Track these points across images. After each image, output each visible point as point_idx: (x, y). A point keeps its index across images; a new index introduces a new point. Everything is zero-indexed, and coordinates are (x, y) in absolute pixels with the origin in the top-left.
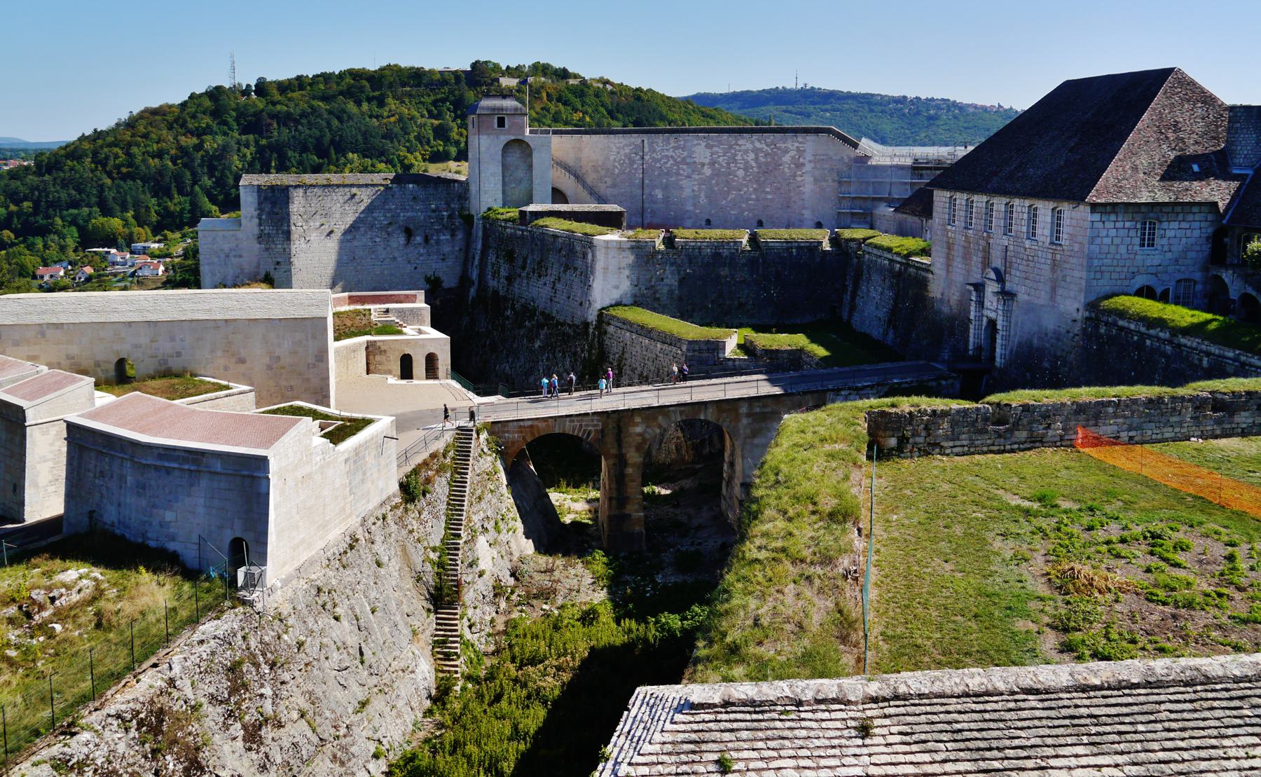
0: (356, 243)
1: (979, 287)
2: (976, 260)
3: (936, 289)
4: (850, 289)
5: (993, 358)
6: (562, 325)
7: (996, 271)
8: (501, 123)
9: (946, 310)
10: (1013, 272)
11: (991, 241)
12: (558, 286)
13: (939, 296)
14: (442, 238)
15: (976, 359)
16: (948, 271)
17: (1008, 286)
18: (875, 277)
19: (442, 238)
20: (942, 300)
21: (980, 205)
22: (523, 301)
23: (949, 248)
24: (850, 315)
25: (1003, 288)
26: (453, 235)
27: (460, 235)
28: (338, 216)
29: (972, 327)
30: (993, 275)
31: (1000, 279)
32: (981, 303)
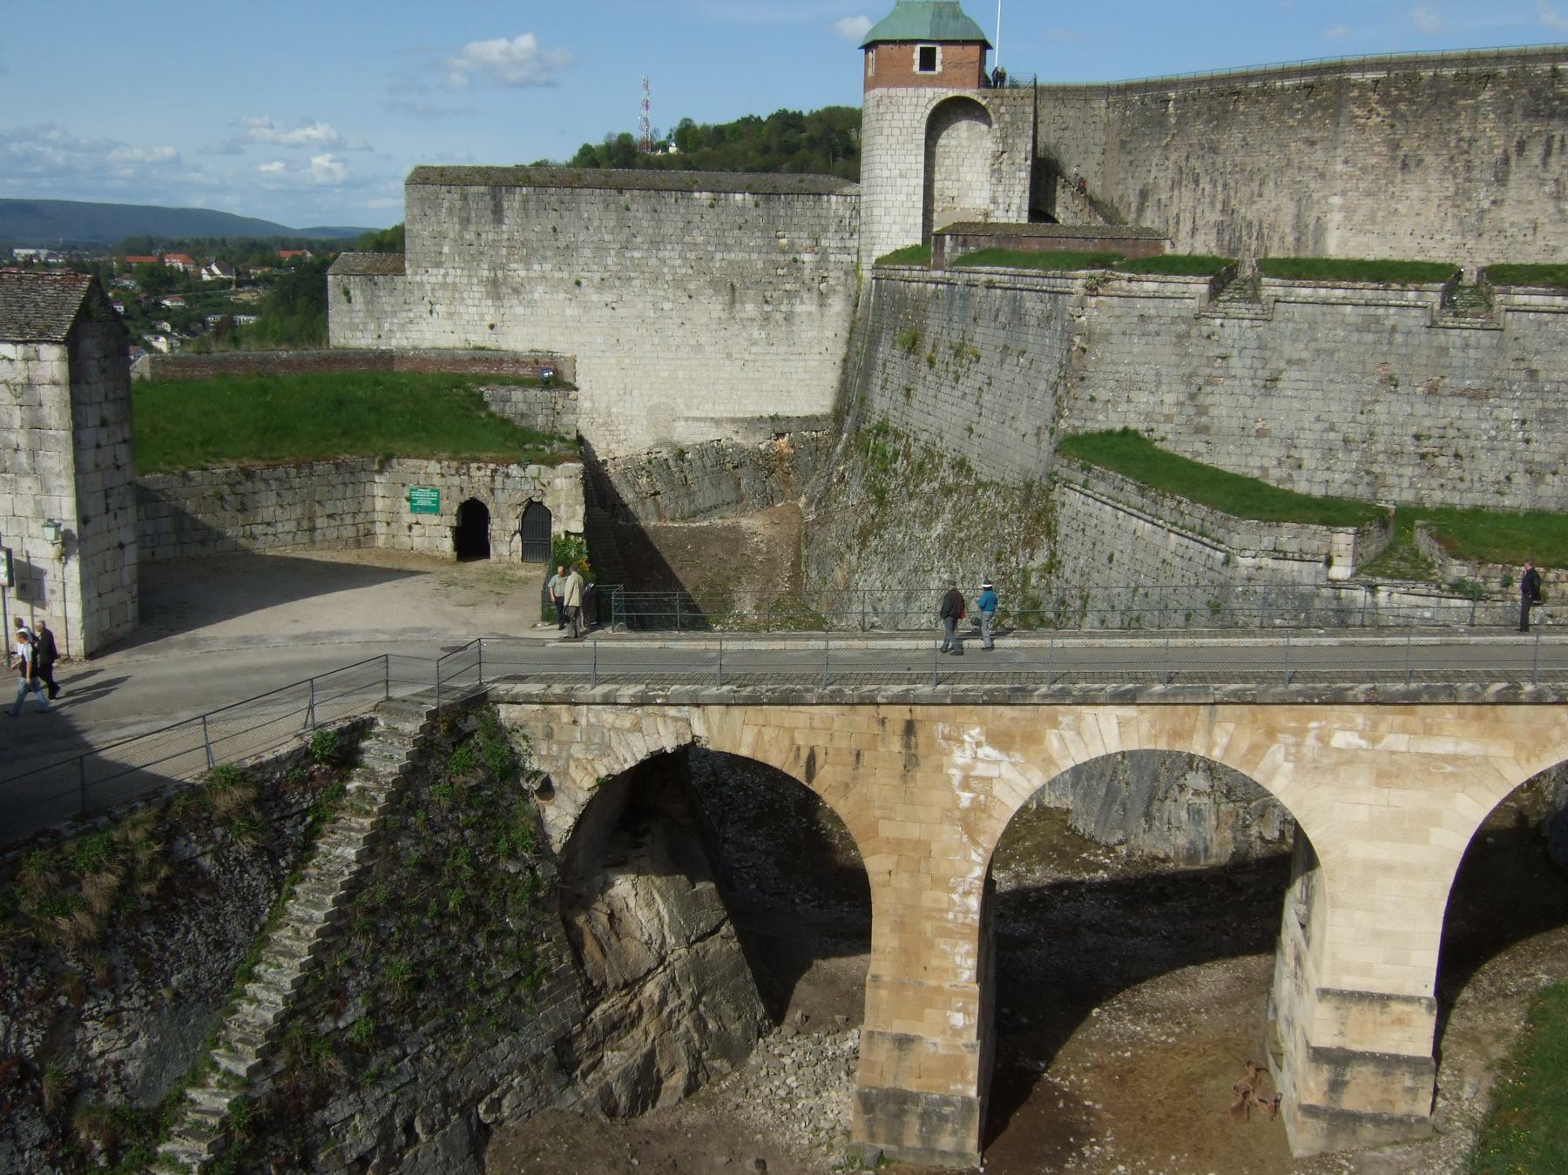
0: (621, 311)
6: (985, 486)
8: (928, 60)
12: (986, 397)
14: (798, 308)
19: (798, 308)
22: (924, 437)
26: (822, 305)
27: (838, 305)
28: (587, 252)
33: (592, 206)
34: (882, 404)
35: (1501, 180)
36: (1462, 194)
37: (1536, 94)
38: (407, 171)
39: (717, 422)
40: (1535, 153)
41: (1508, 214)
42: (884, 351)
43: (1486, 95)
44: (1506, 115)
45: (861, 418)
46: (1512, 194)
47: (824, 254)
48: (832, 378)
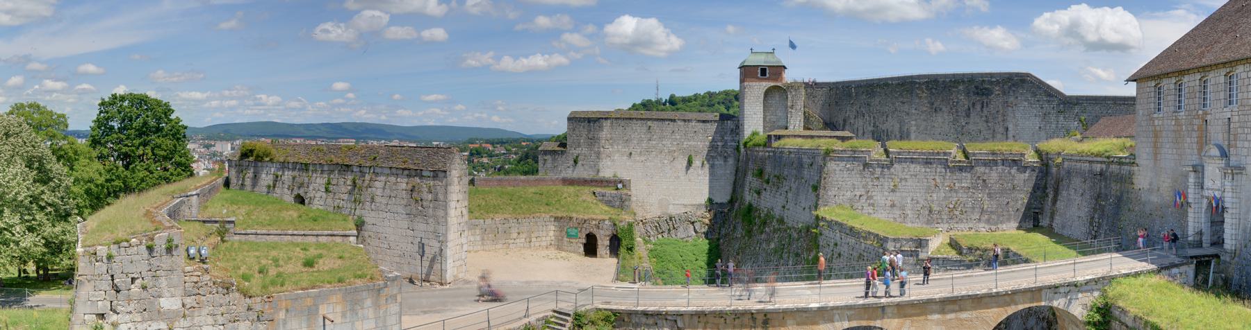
1: (1198, 170)
2: (1190, 142)
3: (1142, 180)
4: (1051, 196)
5: (1218, 242)
7: (1220, 147)
9: (1154, 198)
10: (1239, 144)
11: (1208, 117)
13: (1146, 186)
15: (1199, 244)
16: (1156, 159)
17: (1233, 160)
18: (1077, 182)
20: (1150, 191)
21: (1192, 84)
23: (1156, 136)
24: (1052, 218)
25: (1228, 165)
27: (731, 161)
29: (1190, 210)
30: (1215, 152)
31: (1224, 154)
32: (1201, 186)
33: (638, 129)
34: (748, 197)
35: (968, 116)
36: (955, 121)
37: (977, 87)
38: (567, 114)
39: (685, 206)
40: (978, 107)
41: (971, 127)
42: (749, 178)
43: (961, 87)
44: (968, 94)
45: (742, 203)
46: (971, 121)
47: (726, 142)
48: (729, 189)
